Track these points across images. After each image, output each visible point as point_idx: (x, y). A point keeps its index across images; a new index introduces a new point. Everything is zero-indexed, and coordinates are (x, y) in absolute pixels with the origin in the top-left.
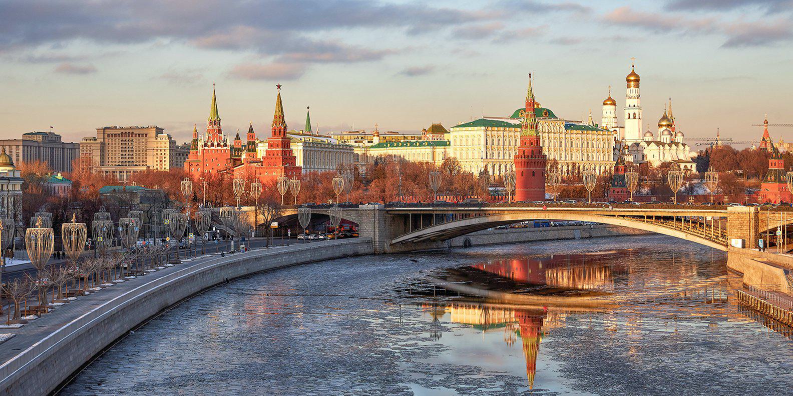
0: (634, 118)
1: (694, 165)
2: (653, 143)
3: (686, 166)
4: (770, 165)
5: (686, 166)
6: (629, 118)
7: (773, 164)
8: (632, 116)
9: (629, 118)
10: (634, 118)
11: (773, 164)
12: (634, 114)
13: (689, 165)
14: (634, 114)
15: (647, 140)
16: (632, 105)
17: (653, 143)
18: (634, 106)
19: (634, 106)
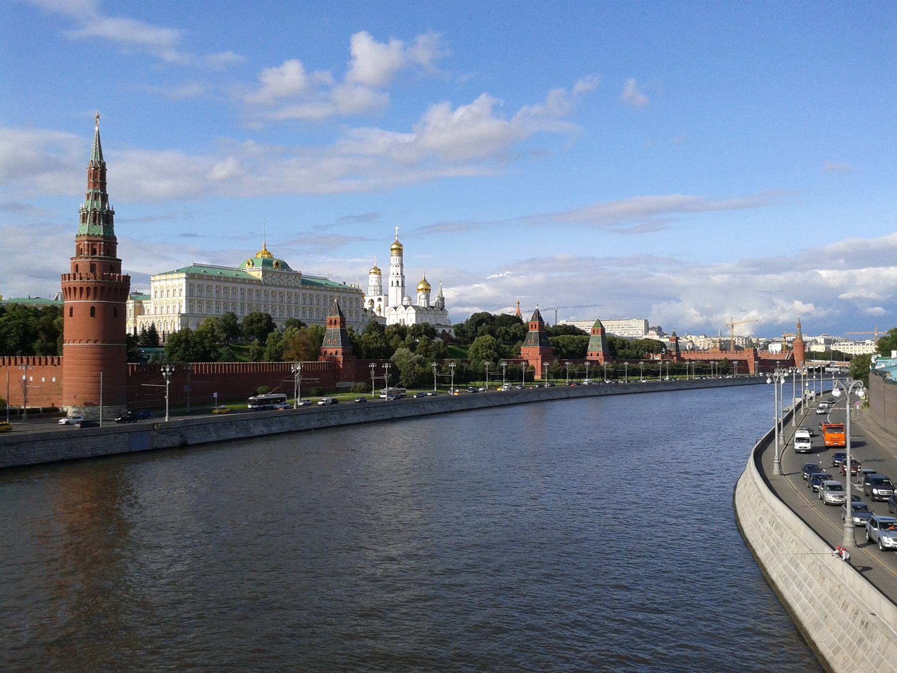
1: (453, 330)
2: (410, 307)
3: (444, 331)
4: (530, 327)
5: (444, 330)
6: (392, 286)
7: (534, 327)
8: (395, 284)
9: (392, 286)
10: (398, 286)
11: (534, 327)
12: (398, 282)
13: (447, 331)
14: (398, 282)
15: (406, 304)
16: (395, 273)
17: (410, 307)
18: (397, 274)
19: (397, 274)
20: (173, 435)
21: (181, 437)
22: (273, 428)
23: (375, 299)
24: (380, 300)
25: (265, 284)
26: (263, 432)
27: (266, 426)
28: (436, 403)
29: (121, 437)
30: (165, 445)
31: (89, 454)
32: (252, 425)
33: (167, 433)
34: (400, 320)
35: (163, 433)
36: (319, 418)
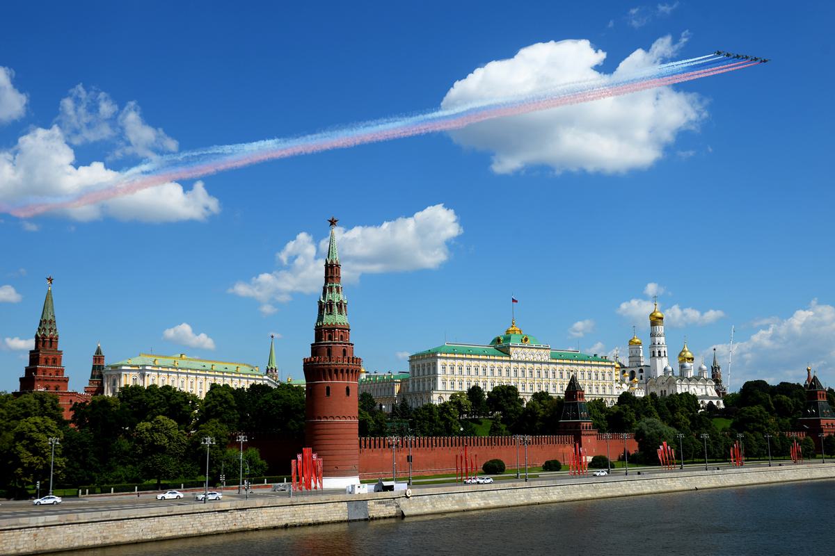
0: (660, 355)
8: (657, 355)
9: (654, 356)
10: (660, 355)
12: (659, 352)
13: (715, 402)
14: (659, 352)
20: (389, 505)
21: (396, 507)
22: (490, 501)
23: (637, 370)
24: (641, 371)
25: (514, 361)
26: (479, 504)
27: (483, 498)
28: (677, 480)
29: (340, 505)
30: (382, 515)
31: (310, 520)
32: (468, 497)
33: (384, 503)
34: (662, 391)
35: (380, 503)
36: (540, 492)
